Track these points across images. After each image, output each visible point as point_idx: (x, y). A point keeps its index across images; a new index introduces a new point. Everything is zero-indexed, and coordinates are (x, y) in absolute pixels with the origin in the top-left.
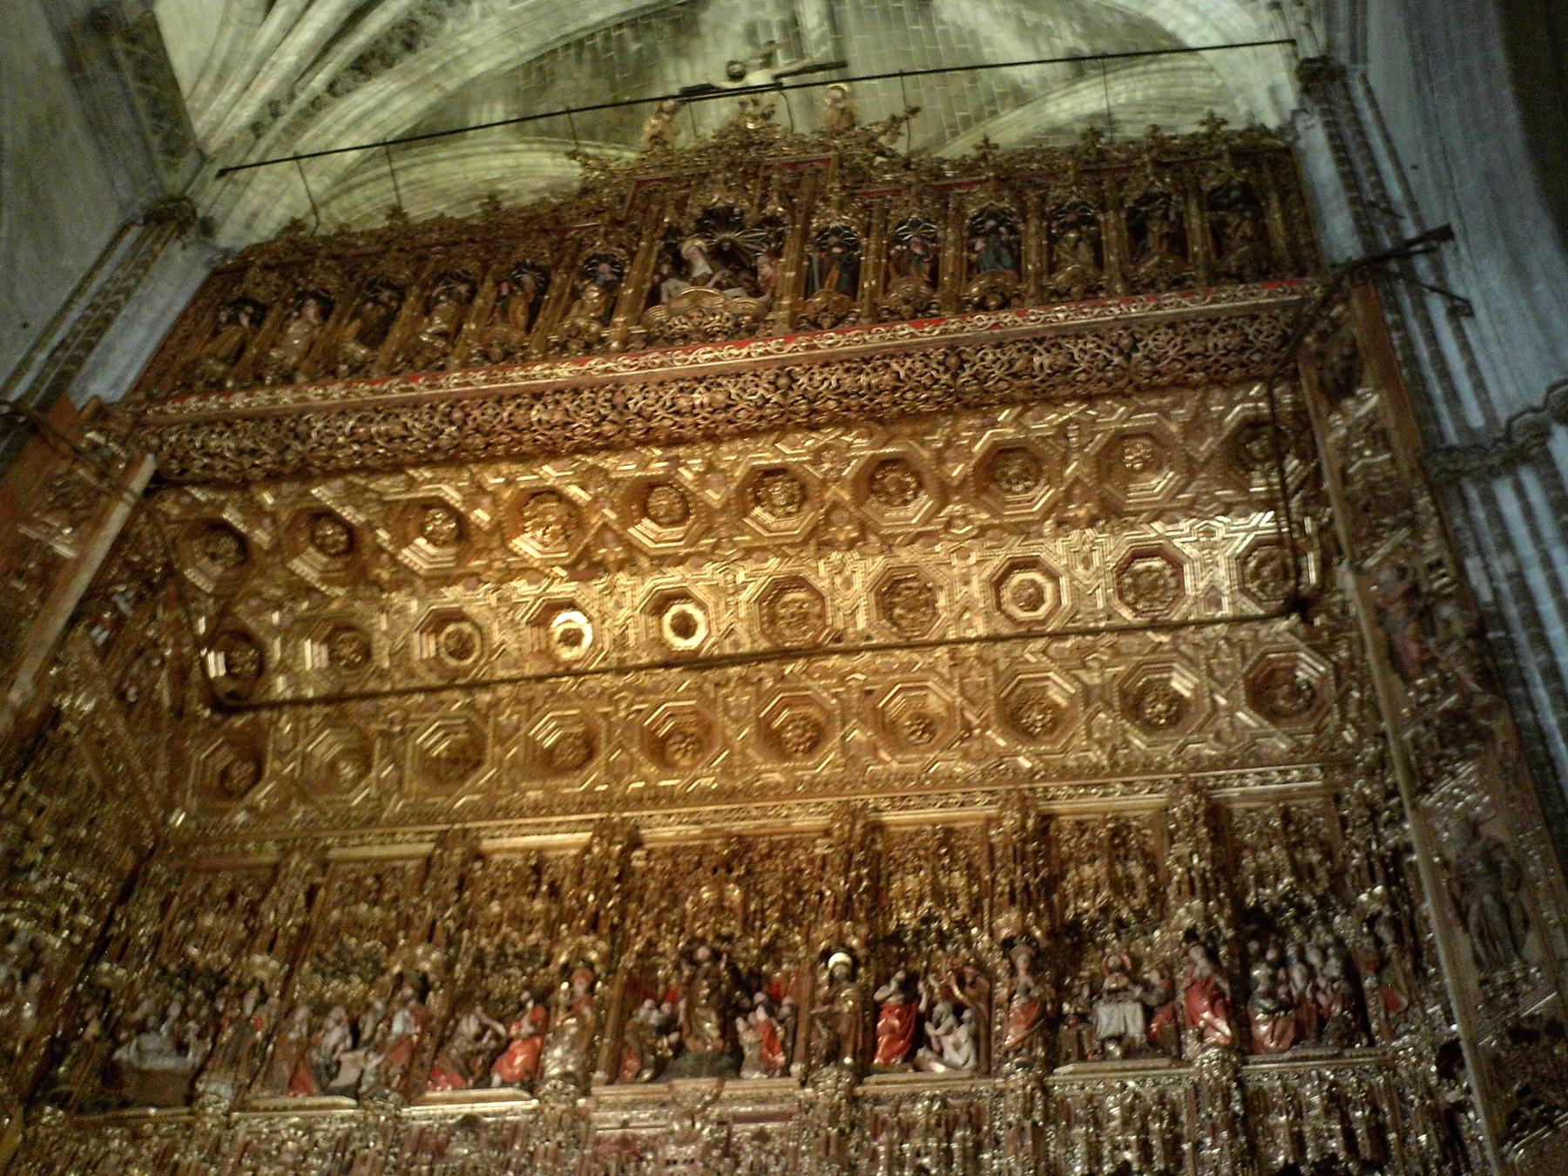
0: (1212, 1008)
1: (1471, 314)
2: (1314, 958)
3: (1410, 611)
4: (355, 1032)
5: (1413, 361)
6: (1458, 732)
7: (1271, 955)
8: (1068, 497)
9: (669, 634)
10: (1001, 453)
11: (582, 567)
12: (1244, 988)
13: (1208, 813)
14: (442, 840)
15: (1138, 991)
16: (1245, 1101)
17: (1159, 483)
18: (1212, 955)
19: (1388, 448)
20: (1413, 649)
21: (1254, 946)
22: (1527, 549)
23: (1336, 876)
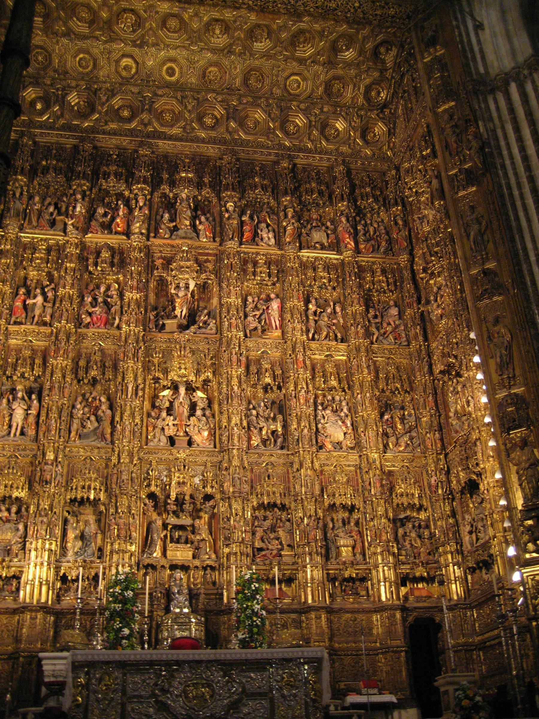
0: (349, 238)
1: (483, 29)
2: (376, 226)
3: (454, 132)
4: (56, 207)
5: (462, 42)
6: (470, 177)
7: (363, 222)
8: (318, 53)
9: (164, 73)
10: (301, 32)
11: (138, 42)
12: (356, 232)
13: (347, 172)
14: (82, 140)
15: (324, 228)
16: (358, 268)
17: (349, 55)
18: (348, 220)
19: (448, 71)
20: (455, 145)
21: (358, 218)
22: (497, 122)
23: (384, 200)
